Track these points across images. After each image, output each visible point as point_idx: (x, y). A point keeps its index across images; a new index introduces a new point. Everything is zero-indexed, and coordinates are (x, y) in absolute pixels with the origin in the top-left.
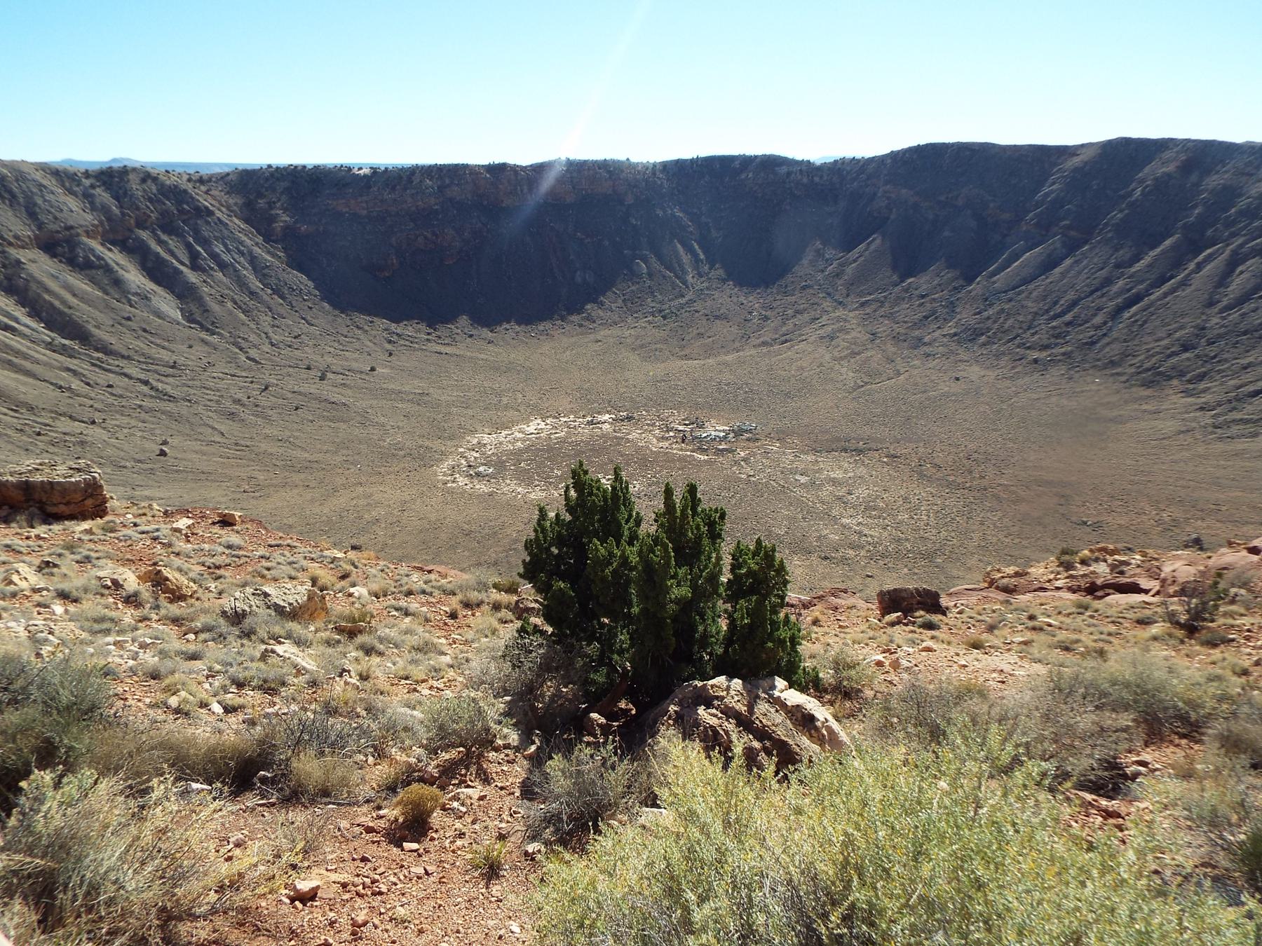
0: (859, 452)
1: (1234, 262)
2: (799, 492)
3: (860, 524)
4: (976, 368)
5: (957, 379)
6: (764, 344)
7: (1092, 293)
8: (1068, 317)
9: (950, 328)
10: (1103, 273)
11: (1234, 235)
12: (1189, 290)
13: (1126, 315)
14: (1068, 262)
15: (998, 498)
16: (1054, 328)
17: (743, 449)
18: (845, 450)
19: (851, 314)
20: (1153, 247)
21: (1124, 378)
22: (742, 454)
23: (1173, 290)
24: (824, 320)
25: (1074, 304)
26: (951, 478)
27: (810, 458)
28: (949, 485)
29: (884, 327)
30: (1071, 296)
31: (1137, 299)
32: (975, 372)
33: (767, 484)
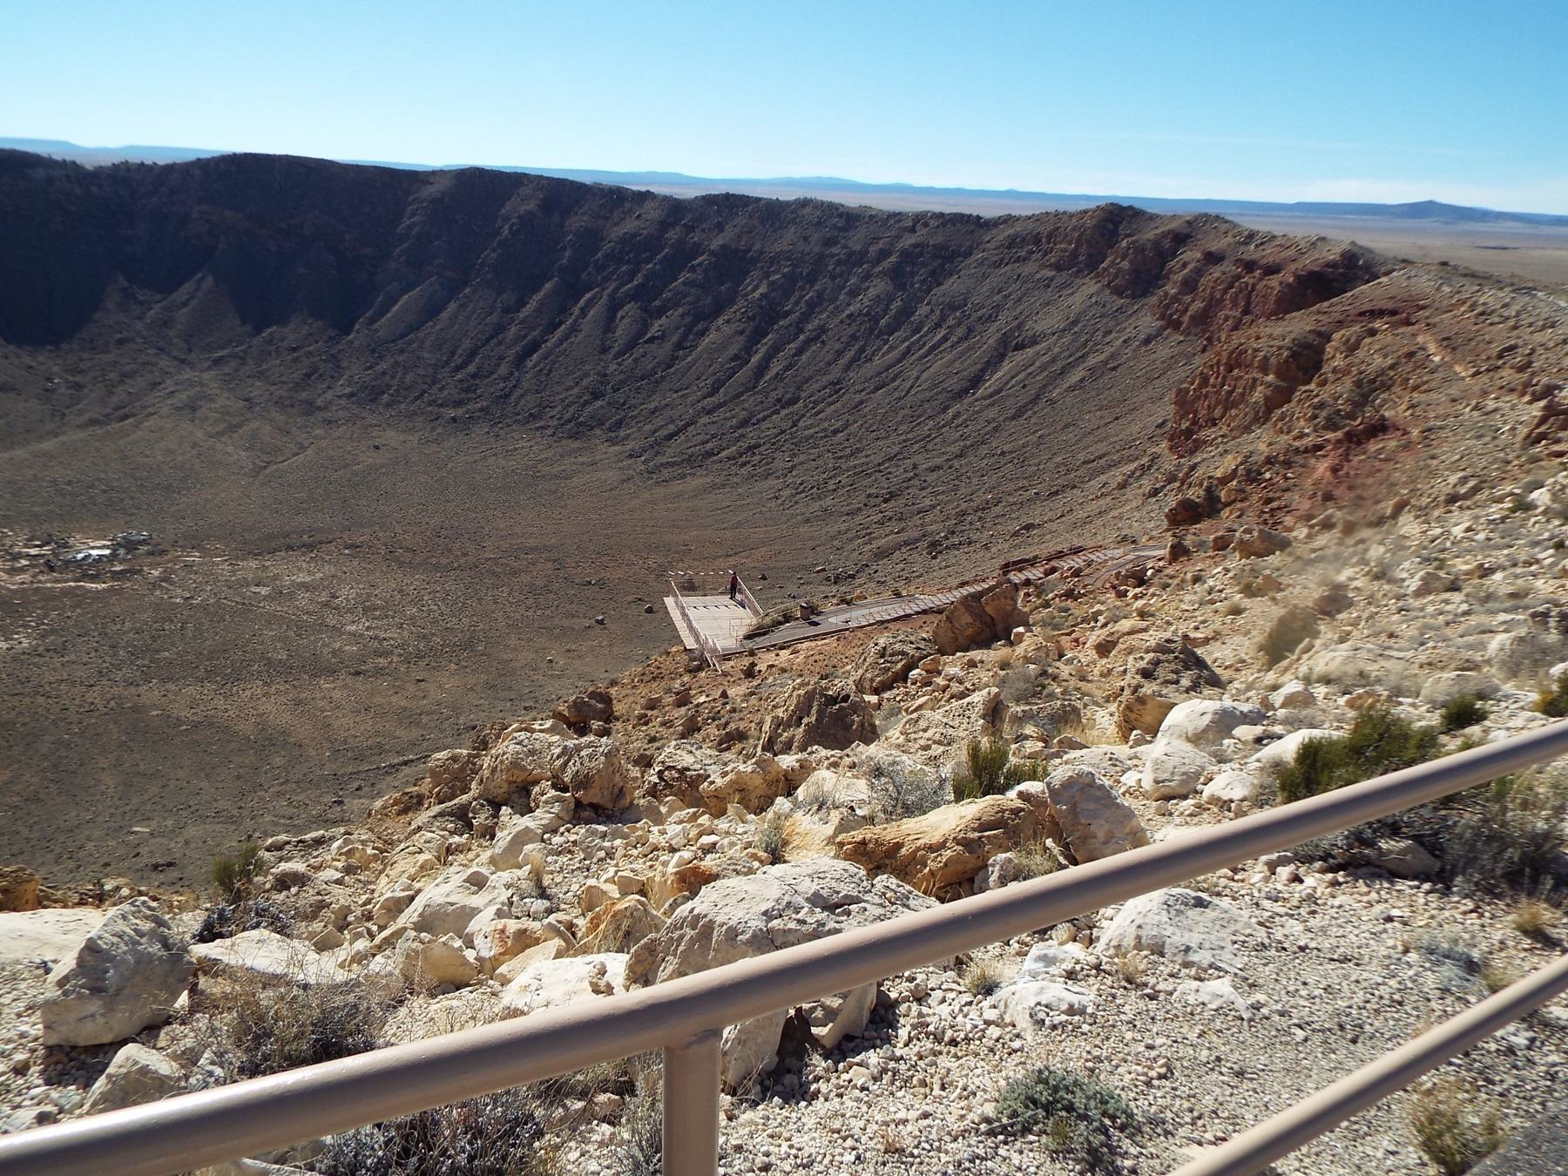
0: (310, 547)
1: (614, 307)
2: (269, 607)
3: (368, 628)
4: (391, 433)
5: (377, 448)
6: (93, 422)
7: (488, 340)
8: (471, 369)
9: (342, 387)
10: (493, 319)
11: (606, 279)
12: (581, 336)
13: (530, 364)
14: (452, 306)
15: (495, 574)
16: (461, 381)
17: (153, 566)
18: (290, 548)
19: (205, 376)
20: (536, 290)
21: (549, 432)
22: (156, 573)
23: (566, 337)
24: (169, 384)
25: (473, 353)
26: (434, 561)
27: (253, 564)
28: (436, 567)
29: (258, 389)
30: (467, 344)
31: (533, 347)
32: (392, 437)
33: (218, 604)
